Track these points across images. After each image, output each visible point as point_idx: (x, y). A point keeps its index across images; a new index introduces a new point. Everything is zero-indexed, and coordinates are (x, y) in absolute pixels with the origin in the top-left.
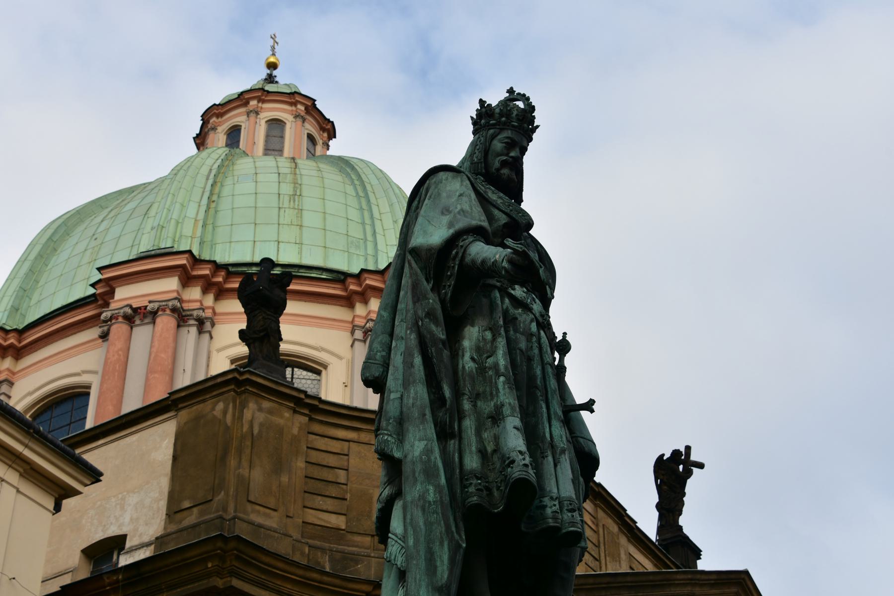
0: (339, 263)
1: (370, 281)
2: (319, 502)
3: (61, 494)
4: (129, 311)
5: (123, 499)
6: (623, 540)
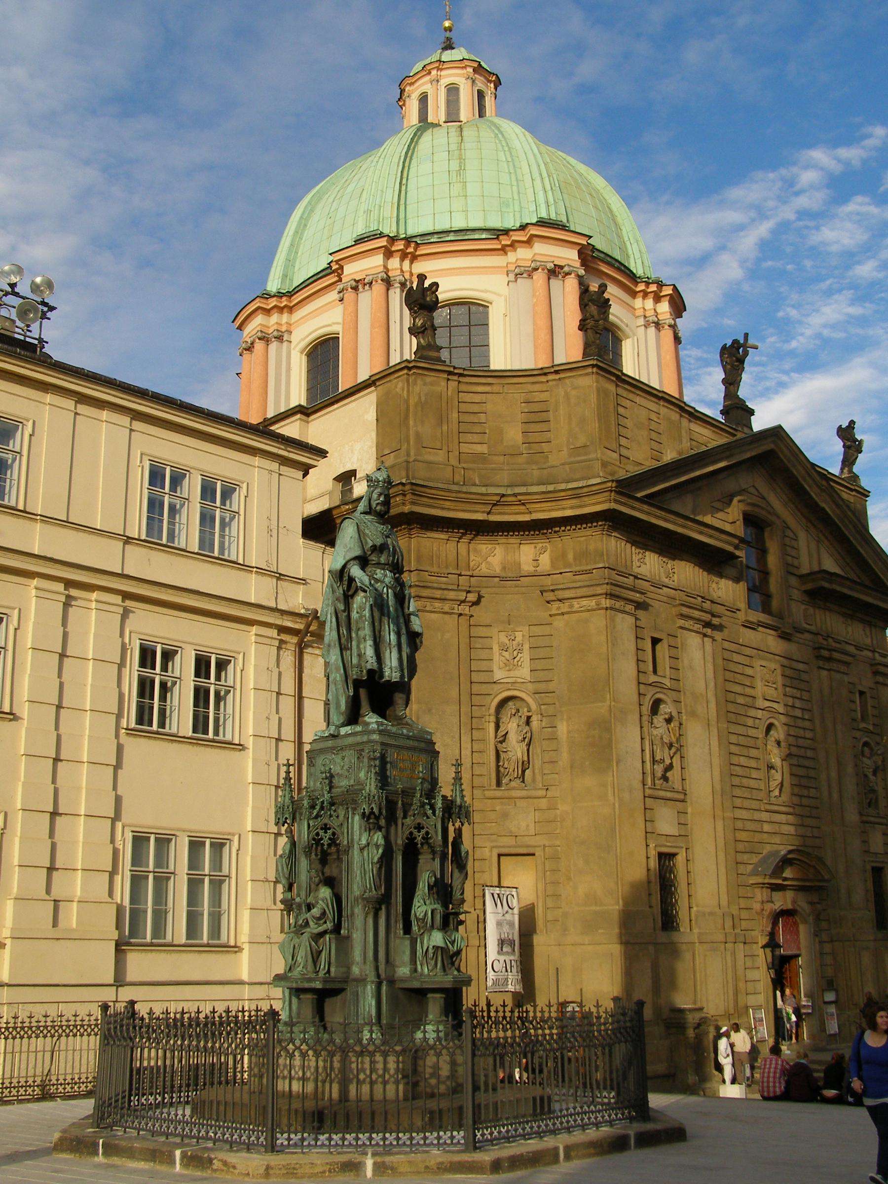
0: (495, 223)
1: (516, 236)
2: (470, 437)
3: (306, 469)
4: (354, 284)
5: (352, 446)
6: (685, 422)
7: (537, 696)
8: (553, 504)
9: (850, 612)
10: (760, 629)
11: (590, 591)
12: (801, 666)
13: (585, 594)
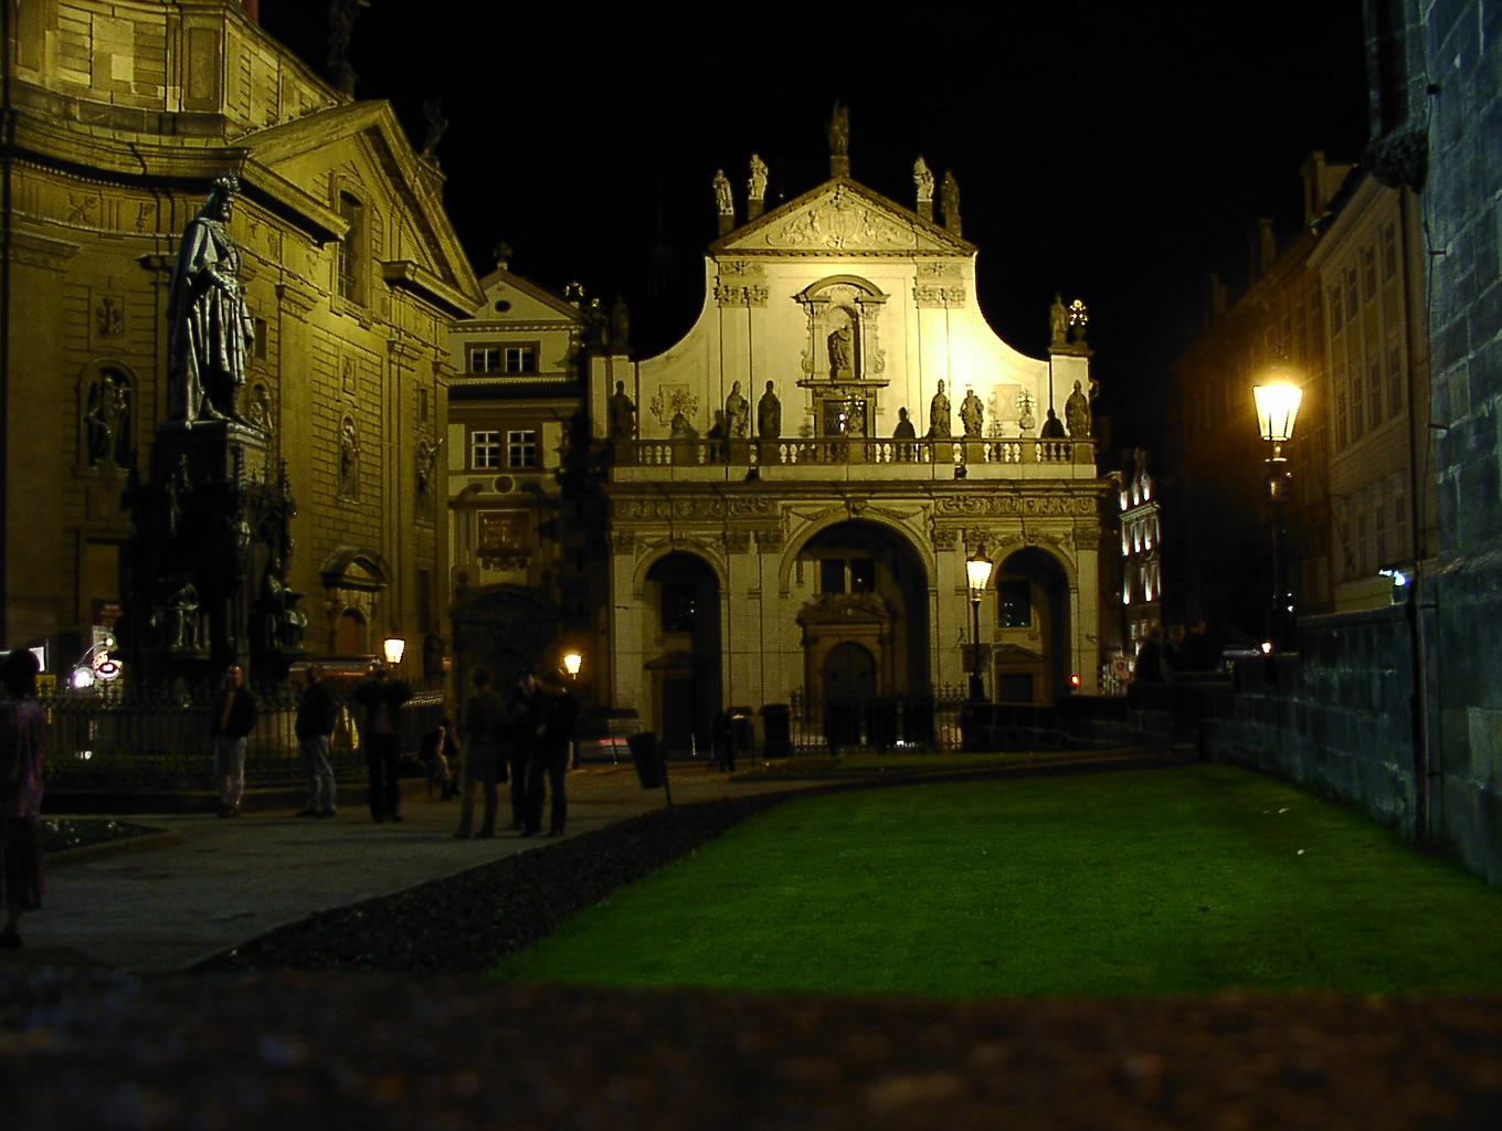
10: (345, 316)
12: (376, 359)
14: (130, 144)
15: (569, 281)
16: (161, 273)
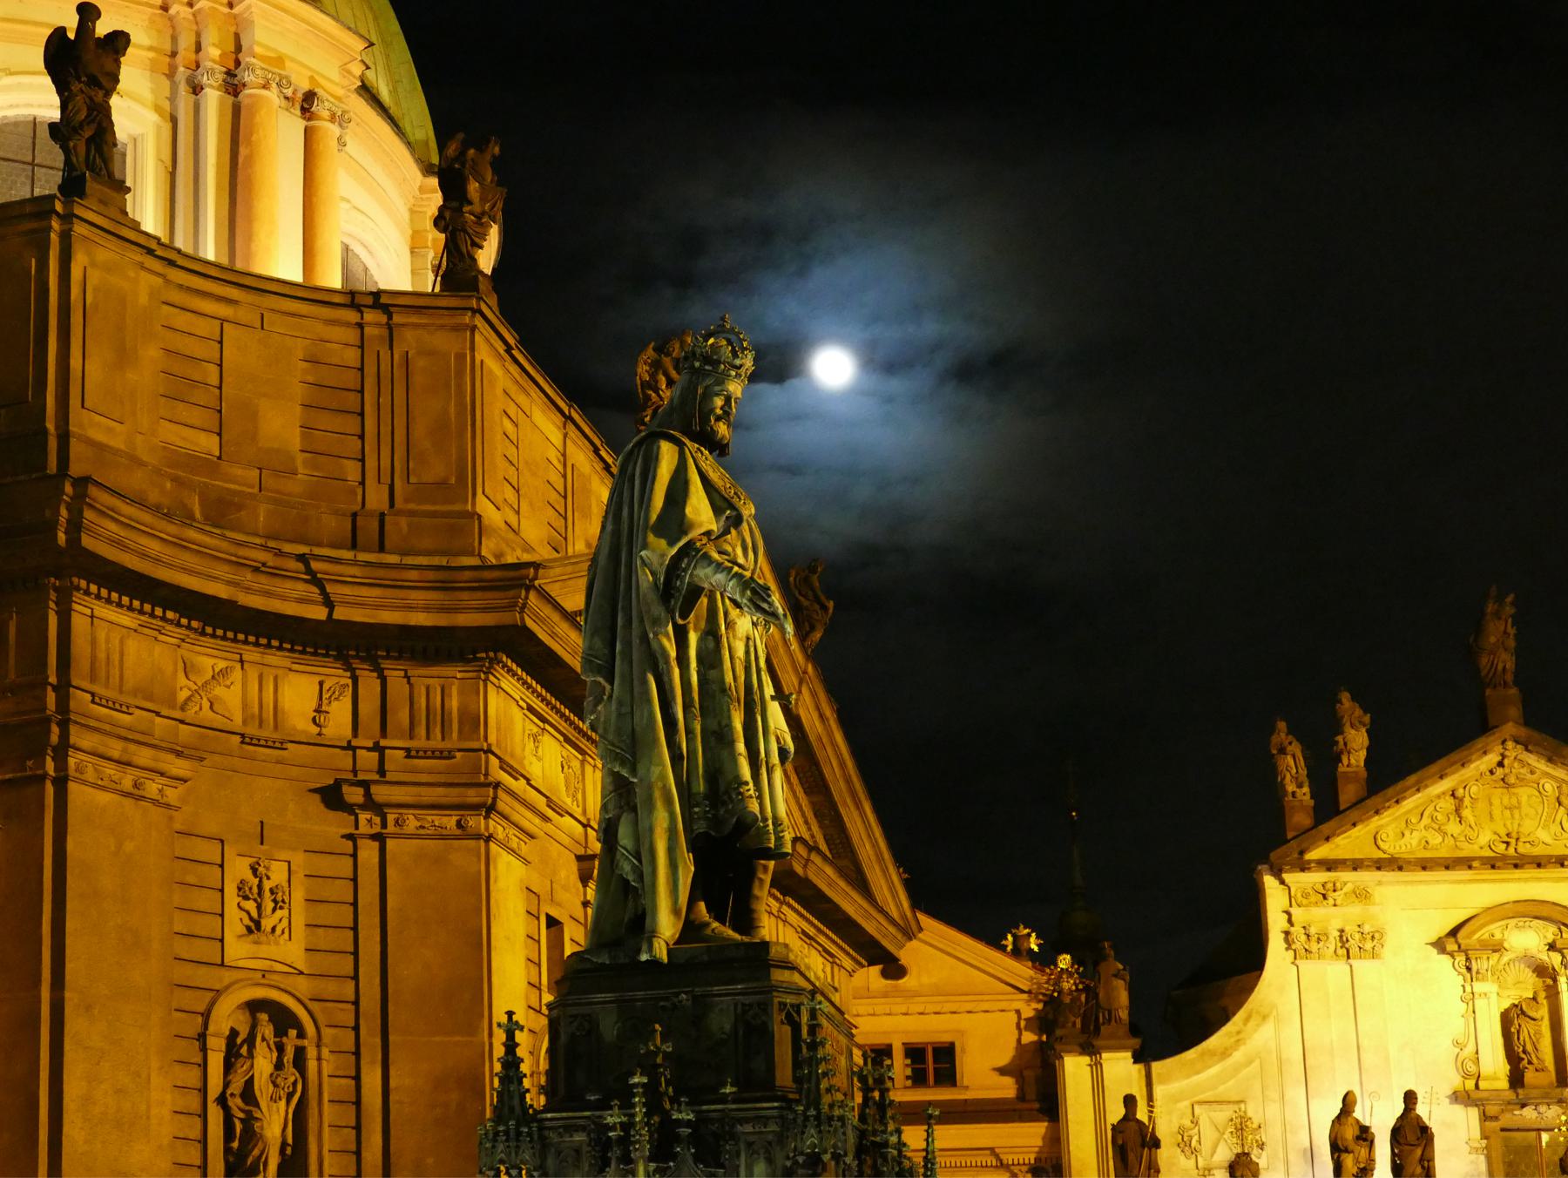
7: (314, 1006)
8: (389, 592)
9: (811, 931)
11: (453, 795)
13: (444, 801)
14: (302, 558)
15: (1012, 925)
16: (364, 817)
